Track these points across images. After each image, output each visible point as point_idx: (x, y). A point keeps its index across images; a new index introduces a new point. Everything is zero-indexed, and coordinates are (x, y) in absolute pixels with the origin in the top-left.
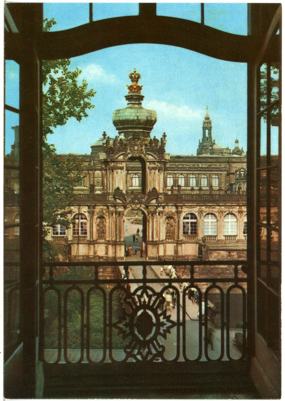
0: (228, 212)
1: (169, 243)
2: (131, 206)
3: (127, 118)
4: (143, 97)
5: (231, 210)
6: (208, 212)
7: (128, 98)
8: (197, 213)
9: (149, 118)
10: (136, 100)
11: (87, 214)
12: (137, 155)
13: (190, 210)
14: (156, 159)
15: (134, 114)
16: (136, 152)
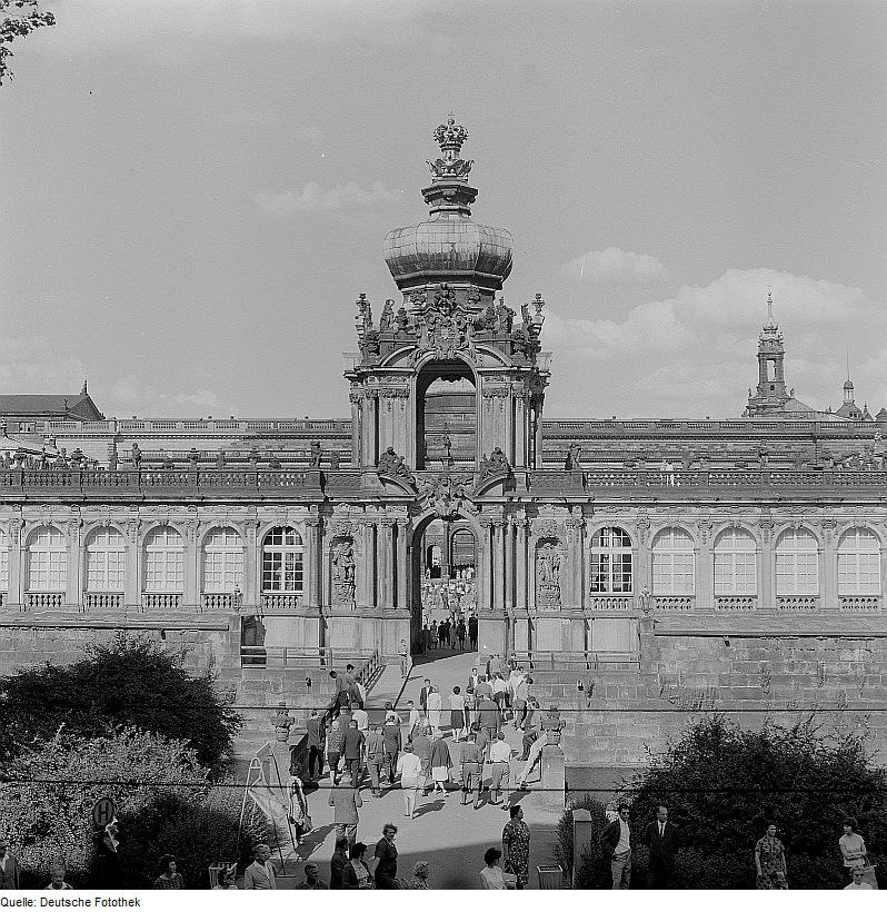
0: (726, 525)
1: (547, 616)
2: (432, 505)
3: (422, 249)
4: (475, 192)
5: (735, 518)
6: (665, 525)
7: (431, 195)
8: (633, 527)
9: (488, 249)
10: (453, 199)
11: (302, 529)
12: (450, 355)
13: (612, 517)
14: (505, 366)
15: (441, 238)
16: (446, 347)
